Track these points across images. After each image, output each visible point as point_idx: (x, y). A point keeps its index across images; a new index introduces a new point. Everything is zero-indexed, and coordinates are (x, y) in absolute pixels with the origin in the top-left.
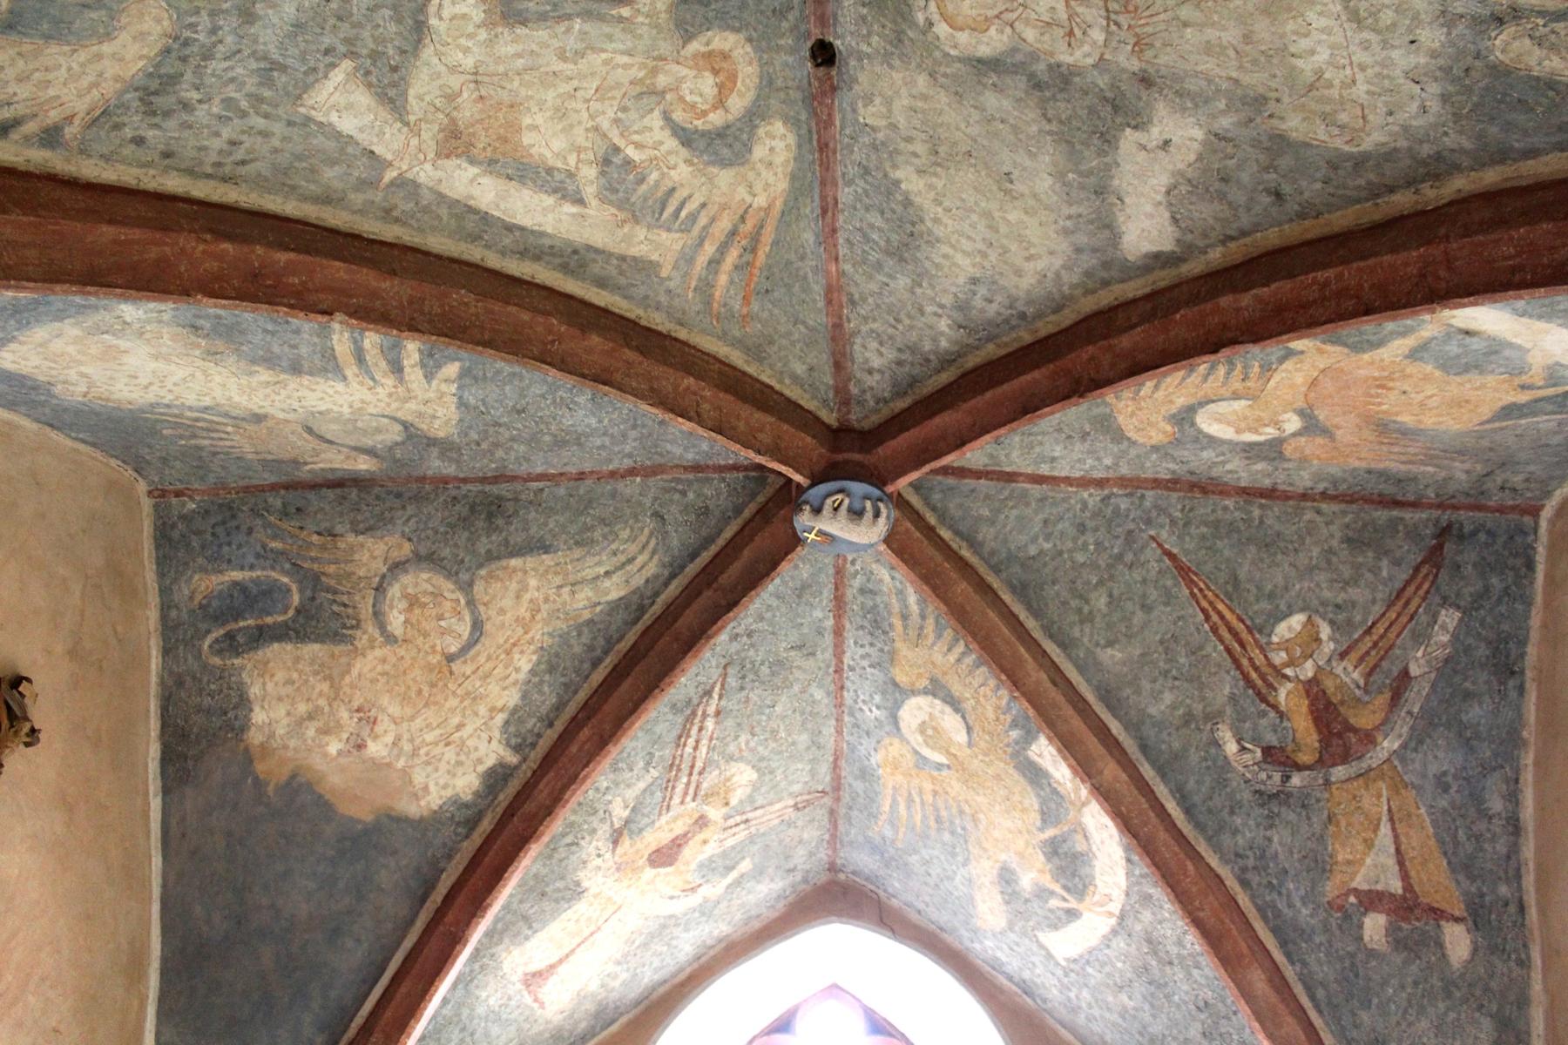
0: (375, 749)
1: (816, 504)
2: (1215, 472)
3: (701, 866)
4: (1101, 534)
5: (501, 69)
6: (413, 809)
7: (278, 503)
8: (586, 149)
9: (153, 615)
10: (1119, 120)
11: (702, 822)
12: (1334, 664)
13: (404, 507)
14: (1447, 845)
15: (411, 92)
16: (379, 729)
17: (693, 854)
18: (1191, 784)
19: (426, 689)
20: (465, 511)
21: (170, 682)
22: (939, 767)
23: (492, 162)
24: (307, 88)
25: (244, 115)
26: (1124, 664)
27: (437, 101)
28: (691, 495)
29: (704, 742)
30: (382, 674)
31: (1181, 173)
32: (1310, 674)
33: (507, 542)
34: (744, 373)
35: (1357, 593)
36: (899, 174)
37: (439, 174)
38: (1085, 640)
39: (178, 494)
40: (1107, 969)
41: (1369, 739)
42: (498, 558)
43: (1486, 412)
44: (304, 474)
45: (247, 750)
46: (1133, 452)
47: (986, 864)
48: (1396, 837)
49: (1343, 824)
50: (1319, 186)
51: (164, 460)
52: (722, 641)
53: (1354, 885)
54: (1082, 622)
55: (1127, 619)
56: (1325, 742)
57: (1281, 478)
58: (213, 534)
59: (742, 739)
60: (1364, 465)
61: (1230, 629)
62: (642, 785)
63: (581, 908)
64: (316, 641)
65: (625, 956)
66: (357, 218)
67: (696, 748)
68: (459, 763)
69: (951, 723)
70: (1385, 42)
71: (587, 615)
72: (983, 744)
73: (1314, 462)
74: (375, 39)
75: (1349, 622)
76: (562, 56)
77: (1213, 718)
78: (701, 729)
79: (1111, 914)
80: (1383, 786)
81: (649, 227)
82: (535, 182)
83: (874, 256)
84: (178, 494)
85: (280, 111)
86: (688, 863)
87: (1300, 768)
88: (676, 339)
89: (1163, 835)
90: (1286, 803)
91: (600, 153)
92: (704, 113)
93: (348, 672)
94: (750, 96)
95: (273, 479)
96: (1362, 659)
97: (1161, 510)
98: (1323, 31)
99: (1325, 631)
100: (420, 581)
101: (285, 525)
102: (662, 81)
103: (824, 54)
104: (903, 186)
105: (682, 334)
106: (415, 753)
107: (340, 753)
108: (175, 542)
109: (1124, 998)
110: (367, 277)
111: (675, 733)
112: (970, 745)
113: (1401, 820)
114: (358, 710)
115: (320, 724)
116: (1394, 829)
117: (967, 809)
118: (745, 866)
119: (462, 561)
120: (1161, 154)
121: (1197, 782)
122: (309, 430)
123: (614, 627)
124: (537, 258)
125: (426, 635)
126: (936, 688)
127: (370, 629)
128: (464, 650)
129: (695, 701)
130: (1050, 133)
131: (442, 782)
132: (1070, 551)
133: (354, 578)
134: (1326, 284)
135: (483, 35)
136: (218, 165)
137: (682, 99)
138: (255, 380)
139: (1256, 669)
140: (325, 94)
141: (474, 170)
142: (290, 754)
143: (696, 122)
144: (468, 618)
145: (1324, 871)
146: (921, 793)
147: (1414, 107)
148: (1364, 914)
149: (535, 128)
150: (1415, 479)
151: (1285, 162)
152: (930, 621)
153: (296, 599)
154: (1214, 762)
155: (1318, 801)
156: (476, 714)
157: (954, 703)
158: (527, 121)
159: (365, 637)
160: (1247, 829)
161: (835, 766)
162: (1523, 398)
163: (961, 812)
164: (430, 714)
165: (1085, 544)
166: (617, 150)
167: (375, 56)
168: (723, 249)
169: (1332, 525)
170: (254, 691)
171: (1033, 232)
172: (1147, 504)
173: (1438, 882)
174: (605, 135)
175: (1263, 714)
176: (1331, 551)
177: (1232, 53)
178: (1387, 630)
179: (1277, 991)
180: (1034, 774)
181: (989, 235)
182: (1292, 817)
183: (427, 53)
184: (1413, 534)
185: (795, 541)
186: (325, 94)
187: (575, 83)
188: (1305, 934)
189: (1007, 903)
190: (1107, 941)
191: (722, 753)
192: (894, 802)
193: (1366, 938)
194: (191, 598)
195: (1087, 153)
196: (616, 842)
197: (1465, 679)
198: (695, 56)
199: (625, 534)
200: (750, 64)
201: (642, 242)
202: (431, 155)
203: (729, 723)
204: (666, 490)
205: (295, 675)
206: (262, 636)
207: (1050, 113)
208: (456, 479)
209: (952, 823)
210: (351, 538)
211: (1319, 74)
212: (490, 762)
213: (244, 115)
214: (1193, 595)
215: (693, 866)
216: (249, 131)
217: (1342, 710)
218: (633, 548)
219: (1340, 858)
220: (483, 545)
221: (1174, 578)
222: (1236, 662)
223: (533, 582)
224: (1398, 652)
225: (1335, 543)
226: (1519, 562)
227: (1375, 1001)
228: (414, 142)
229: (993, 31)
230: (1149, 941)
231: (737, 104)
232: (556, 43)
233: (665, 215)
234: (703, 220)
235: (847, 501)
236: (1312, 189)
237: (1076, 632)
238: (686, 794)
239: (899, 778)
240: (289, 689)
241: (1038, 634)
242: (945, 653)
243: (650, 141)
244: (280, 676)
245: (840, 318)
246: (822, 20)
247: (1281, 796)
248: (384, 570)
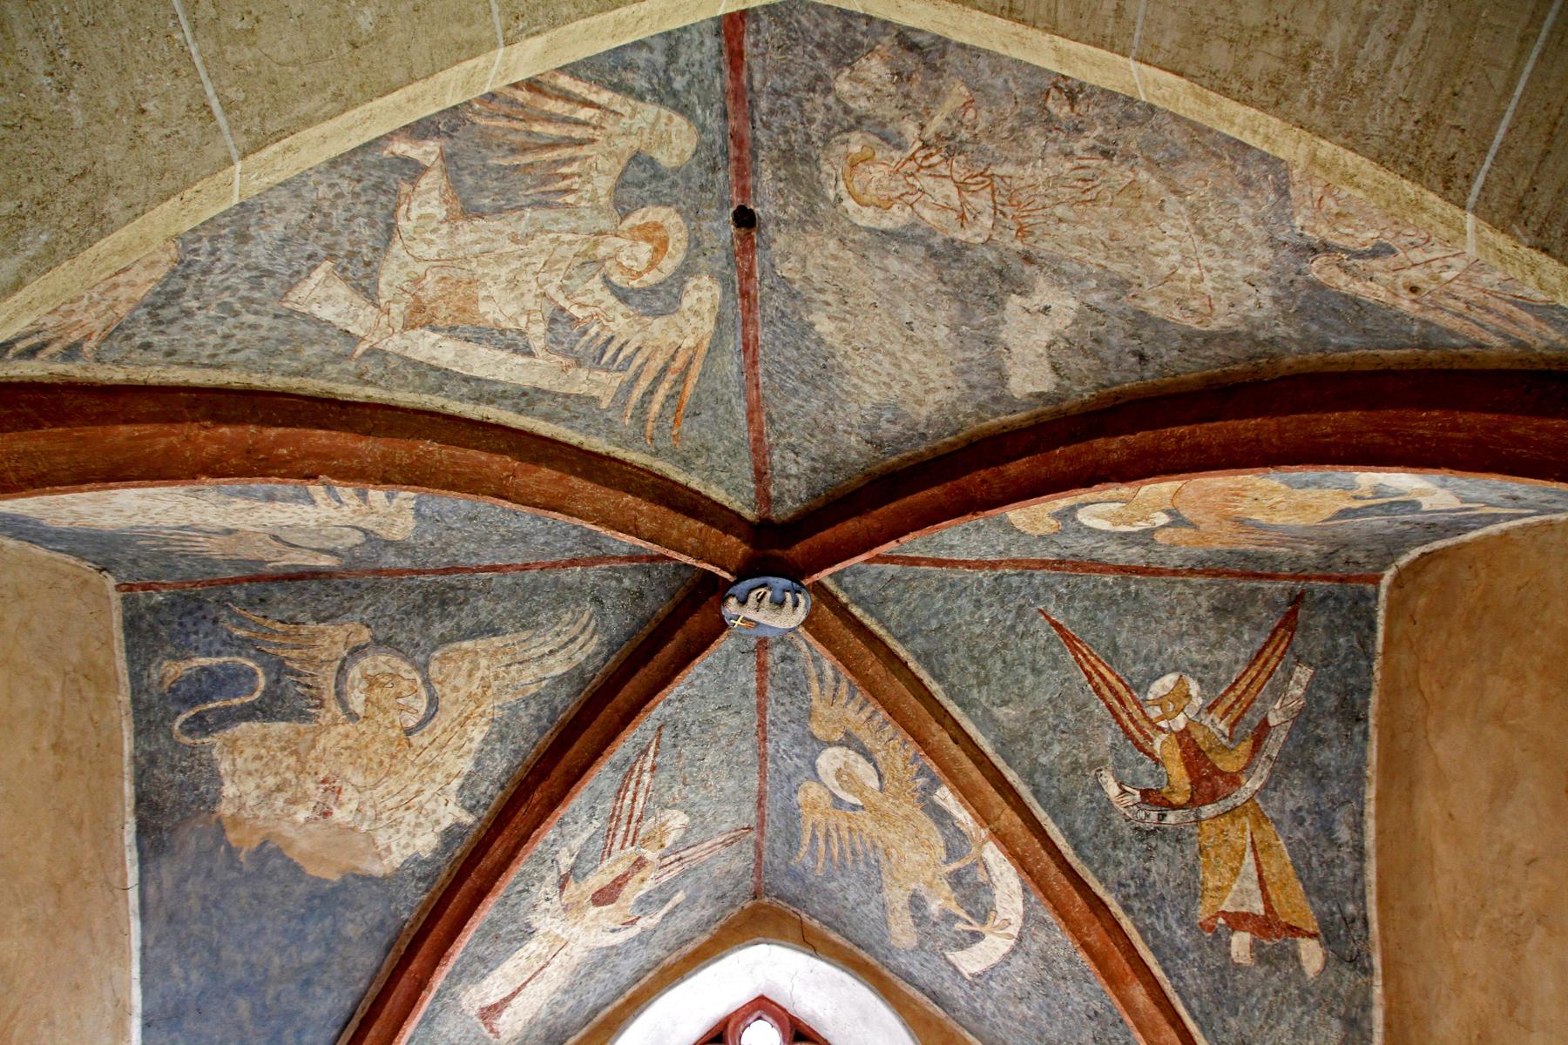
0: (339, 815)
1: (742, 597)
2: (1095, 555)
3: (640, 901)
4: (996, 608)
5: (460, 254)
6: (377, 869)
7: (242, 595)
9: (125, 697)
10: (1005, 287)
11: (640, 863)
12: (1203, 716)
13: (361, 597)
14: (1302, 869)
15: (382, 281)
16: (344, 797)
17: (632, 892)
18: (1078, 825)
19: (387, 761)
20: (420, 600)
21: (143, 760)
22: (854, 807)
23: (452, 329)
24: (291, 287)
25: (237, 314)
26: (1017, 720)
28: (627, 583)
29: (641, 794)
30: (346, 748)
31: (1060, 333)
32: (1182, 726)
33: (459, 628)
34: (675, 483)
35: (1223, 656)
36: (812, 318)
37: (408, 343)
38: (983, 700)
39: (145, 587)
40: (1008, 983)
41: (1234, 780)
42: (451, 641)
43: (1327, 513)
44: (268, 568)
45: (219, 821)
46: (1022, 540)
47: (898, 892)
48: (1258, 865)
49: (1212, 855)
50: (1175, 353)
51: (134, 562)
52: (659, 710)
53: (1222, 908)
54: (979, 685)
55: (1019, 681)
56: (1196, 782)
57: (1153, 558)
58: (181, 624)
59: (675, 790)
60: (1226, 548)
61: (1111, 689)
62: (586, 835)
63: (532, 946)
64: (282, 720)
65: (572, 985)
66: (332, 385)
67: (634, 800)
68: (418, 825)
69: (863, 769)
70: (1226, 253)
71: (533, 689)
72: (892, 789)
73: (1178, 547)
74: (352, 244)
75: (1215, 680)
76: (514, 239)
77: (1098, 765)
78: (638, 783)
79: (1010, 936)
80: (1245, 819)
82: (488, 341)
83: (790, 384)
84: (145, 587)
85: (268, 308)
86: (627, 900)
87: (1174, 807)
88: (615, 459)
89: (1053, 870)
90: (1162, 838)
91: (548, 314)
92: (640, 274)
93: (313, 747)
94: (680, 257)
95: (237, 574)
96: (1226, 713)
97: (1049, 587)
98: (1175, 238)
99: (1194, 688)
100: (379, 662)
101: (250, 614)
102: (602, 251)
103: (745, 219)
104: (817, 328)
105: (620, 453)
106: (377, 819)
107: (308, 820)
108: (142, 633)
109: (1023, 1007)
110: (344, 440)
111: (616, 787)
112: (881, 790)
113: (1263, 851)
114: (324, 782)
115: (288, 795)
116: (1256, 859)
117: (879, 844)
118: (679, 897)
119: (418, 645)
120: (1042, 316)
121: (1084, 822)
122: (276, 538)
123: (558, 700)
124: (490, 402)
125: (386, 711)
126: (849, 741)
127: (333, 708)
128: (421, 724)
129: (633, 759)
130: (945, 293)
131: (403, 842)
132: (968, 624)
133: (316, 662)
134: (1181, 438)
135: (445, 228)
136: (214, 356)
137: (620, 264)
138: (231, 508)
139: (1134, 722)
140: (307, 290)
141: (436, 336)
142: (260, 823)
144: (423, 694)
145: (1196, 896)
146: (838, 829)
147: (1251, 302)
148: (1232, 934)
149: (489, 298)
150: (1271, 557)
151: (1147, 333)
152: (844, 686)
153: (262, 682)
154: (1099, 803)
155: (1191, 835)
156: (433, 781)
157: (868, 755)
159: (329, 715)
160: (1129, 859)
161: (760, 805)
162: (1357, 504)
163: (875, 847)
164: (392, 784)
165: (982, 617)
166: (563, 310)
167: (351, 255)
168: (657, 380)
169: (1201, 596)
170: (224, 766)
171: (932, 371)
172: (1037, 581)
173: (1296, 906)
175: (1142, 762)
176: (1198, 619)
177: (1101, 247)
178: (1248, 686)
179: (1157, 1003)
180: (940, 816)
181: (893, 370)
182: (1167, 850)
183: (397, 247)
184: (1271, 604)
185: (722, 626)
186: (307, 290)
187: (526, 260)
188: (1180, 952)
189: (918, 925)
190: (1006, 960)
191: (657, 803)
192: (814, 837)
193: (1234, 955)
194: (161, 683)
195: (978, 312)
196: (562, 887)
197: (1317, 726)
198: (631, 229)
199: (567, 617)
200: (680, 230)
201: (583, 382)
203: (664, 776)
204: (605, 578)
205: (263, 751)
206: (228, 718)
207: (946, 278)
208: (411, 571)
209: (866, 855)
210: (312, 625)
211: (1174, 269)
212: (447, 823)
213: (237, 314)
214: (1076, 658)
215: (632, 902)
216: (241, 326)
217: (1210, 756)
218: (575, 630)
219: (1210, 885)
220: (437, 629)
221: (1060, 645)
222: (1115, 715)
223: (483, 662)
224: (1258, 704)
225: (1202, 612)
226: (1362, 624)
227: (1242, 1008)
228: (385, 319)
229: (895, 207)
230: (1044, 959)
231: (668, 265)
232: (509, 230)
233: (605, 359)
234: (638, 361)
235: (769, 594)
236: (1170, 355)
237: (975, 693)
238: (625, 840)
239: (818, 816)
240: (257, 765)
241: (941, 696)
242: (857, 714)
243: (590, 299)
244: (250, 752)
245: (761, 433)
246: (744, 191)
247: (1159, 832)
248: (345, 654)
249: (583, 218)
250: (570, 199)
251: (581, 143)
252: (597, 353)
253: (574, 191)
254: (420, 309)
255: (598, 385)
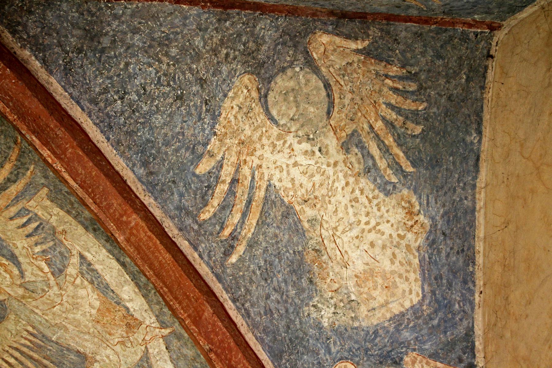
8: (69, 282)
15: (138, 358)
23: (119, 304)
27: (129, 345)
37: (144, 313)
76: (66, 329)
81: (48, 222)
91: (63, 277)
102: (21, 291)
135: (98, 358)
141: (129, 305)
143: (7, 263)
158: (94, 312)
166: (53, 274)
174: (57, 284)
187: (64, 315)
201: (56, 216)
202: (144, 326)
228: (147, 338)
234: (13, 210)
249: (26, 316)
250: (30, 329)
251: (17, 349)
252: (40, 231)
253: (27, 331)
254: (128, 325)
255: (45, 208)
